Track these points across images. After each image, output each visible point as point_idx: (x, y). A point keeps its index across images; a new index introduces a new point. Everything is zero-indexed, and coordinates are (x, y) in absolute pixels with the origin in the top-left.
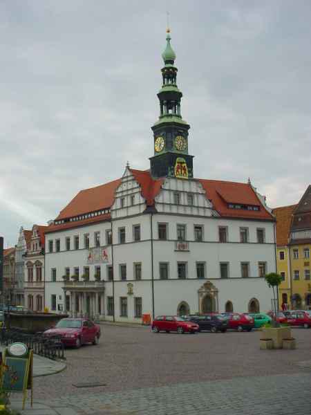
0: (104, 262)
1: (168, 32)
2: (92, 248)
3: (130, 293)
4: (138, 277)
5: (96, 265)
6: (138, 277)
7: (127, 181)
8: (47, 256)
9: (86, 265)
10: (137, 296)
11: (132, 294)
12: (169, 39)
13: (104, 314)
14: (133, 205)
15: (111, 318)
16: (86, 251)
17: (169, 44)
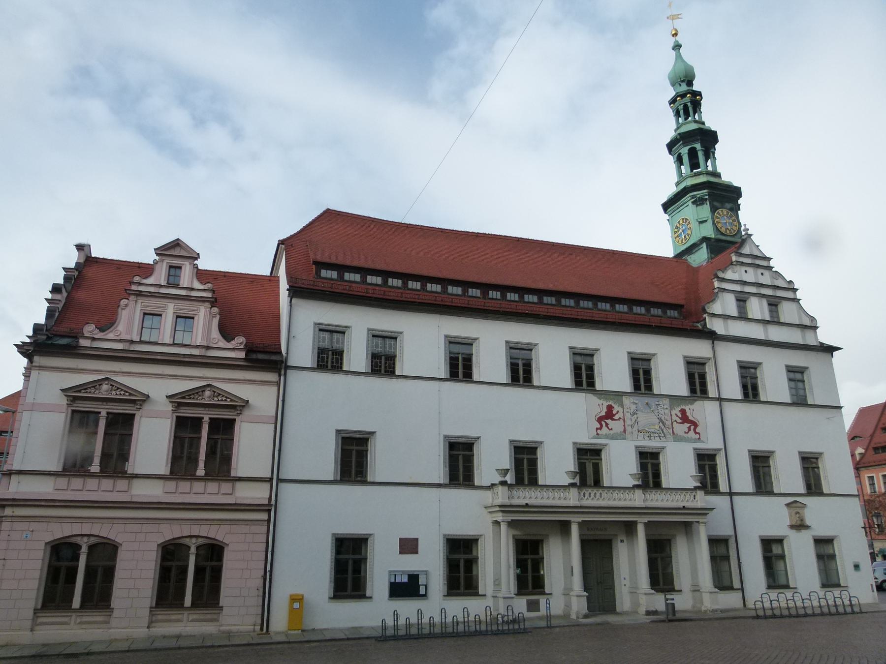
0: (677, 439)
1: (676, 35)
2: (618, 395)
3: (800, 526)
4: (814, 487)
5: (650, 444)
6: (814, 487)
7: (758, 266)
8: (297, 382)
9: (586, 438)
10: (823, 532)
11: (807, 527)
12: (677, 47)
13: (696, 589)
14: (775, 321)
15: (730, 600)
16: (581, 398)
17: (679, 57)
